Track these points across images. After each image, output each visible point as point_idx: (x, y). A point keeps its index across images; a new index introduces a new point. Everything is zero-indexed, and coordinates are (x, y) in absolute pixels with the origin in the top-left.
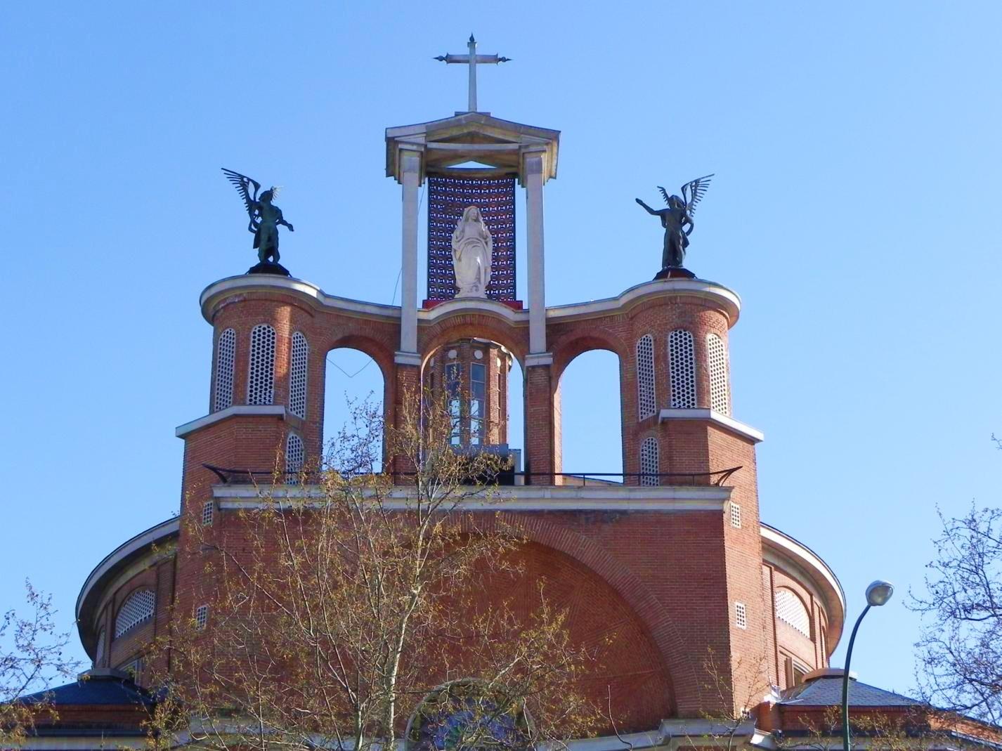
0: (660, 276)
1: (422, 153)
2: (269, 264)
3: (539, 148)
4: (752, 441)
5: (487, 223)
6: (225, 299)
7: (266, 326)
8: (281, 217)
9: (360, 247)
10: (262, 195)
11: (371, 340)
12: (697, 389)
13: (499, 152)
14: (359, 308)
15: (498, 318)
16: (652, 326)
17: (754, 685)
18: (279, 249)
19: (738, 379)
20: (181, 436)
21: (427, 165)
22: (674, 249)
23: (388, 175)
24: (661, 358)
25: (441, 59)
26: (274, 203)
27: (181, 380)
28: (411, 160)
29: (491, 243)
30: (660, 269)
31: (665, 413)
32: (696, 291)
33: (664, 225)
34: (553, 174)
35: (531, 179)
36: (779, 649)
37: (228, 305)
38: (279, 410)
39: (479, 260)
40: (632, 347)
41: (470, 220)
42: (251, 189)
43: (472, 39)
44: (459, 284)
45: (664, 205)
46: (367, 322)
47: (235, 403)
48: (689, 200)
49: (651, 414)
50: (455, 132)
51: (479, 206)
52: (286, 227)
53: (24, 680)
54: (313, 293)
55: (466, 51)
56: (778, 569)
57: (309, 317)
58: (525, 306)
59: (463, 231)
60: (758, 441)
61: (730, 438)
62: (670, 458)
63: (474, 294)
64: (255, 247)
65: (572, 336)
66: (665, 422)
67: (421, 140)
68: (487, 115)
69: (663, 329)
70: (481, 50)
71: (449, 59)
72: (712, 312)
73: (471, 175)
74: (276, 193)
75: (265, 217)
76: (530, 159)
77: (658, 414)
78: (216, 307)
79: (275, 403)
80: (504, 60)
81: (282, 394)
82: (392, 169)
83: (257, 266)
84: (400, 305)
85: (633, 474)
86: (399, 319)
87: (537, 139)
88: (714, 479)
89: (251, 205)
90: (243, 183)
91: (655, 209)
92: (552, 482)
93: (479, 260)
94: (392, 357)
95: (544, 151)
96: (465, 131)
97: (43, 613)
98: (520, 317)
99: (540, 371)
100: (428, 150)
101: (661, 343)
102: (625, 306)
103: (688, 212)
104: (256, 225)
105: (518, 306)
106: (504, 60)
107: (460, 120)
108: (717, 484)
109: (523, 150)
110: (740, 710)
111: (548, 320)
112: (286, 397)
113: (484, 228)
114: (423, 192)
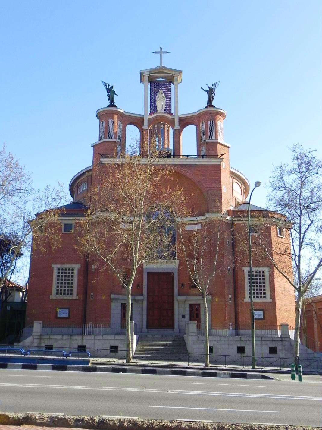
0: (207, 107)
1: (149, 77)
2: (112, 105)
3: (177, 75)
4: (228, 147)
5: (164, 94)
6: (102, 113)
7: (111, 120)
8: (115, 93)
9: (134, 100)
10: (110, 87)
11: (136, 123)
12: (215, 134)
13: (167, 76)
14: (134, 115)
15: (167, 118)
16: (204, 119)
17: (227, 205)
18: (115, 101)
19: (224, 132)
20: (92, 146)
21: (150, 80)
22: (210, 100)
23: (140, 82)
24: (206, 127)
25: (153, 52)
26: (113, 89)
27: (92, 133)
28: (146, 79)
29: (165, 99)
30: (207, 105)
31: (207, 141)
32: (215, 111)
33: (208, 94)
34: (181, 81)
35: (175, 83)
36: (233, 197)
37: (102, 115)
38: (115, 140)
39: (162, 103)
40: (199, 124)
41: (160, 94)
42: (108, 86)
43: (161, 47)
44: (158, 109)
45: (208, 89)
46: (136, 119)
47: (105, 138)
48: (214, 88)
49: (204, 141)
50: (157, 71)
51: (163, 90)
52: (116, 95)
53: (58, 204)
54: (123, 112)
55: (159, 50)
56: (234, 178)
57: (122, 118)
58: (174, 115)
59: (159, 96)
60: (230, 147)
61: (223, 147)
62: (208, 152)
63: (161, 112)
64: (109, 100)
65: (185, 122)
66: (207, 143)
67: (149, 73)
68: (164, 67)
69: (207, 120)
70: (163, 50)
71: (155, 52)
72: (219, 116)
73: (160, 82)
74: (113, 87)
75: (111, 93)
76: (175, 78)
77: (206, 141)
78: (100, 115)
79: (114, 138)
80: (169, 52)
81: (116, 136)
82: (142, 81)
83: (109, 105)
84: (143, 114)
85: (199, 155)
86: (143, 118)
87: (177, 73)
88: (219, 157)
89: (108, 90)
90: (106, 84)
91: (206, 90)
92: (180, 157)
93: (162, 103)
94: (142, 127)
95: (179, 76)
96: (159, 71)
97: (62, 188)
98: (173, 117)
99: (177, 130)
101: (206, 124)
102: (198, 114)
103: (214, 91)
104: (109, 95)
105: (172, 114)
106: (169, 52)
107: (158, 68)
108: (219, 158)
109: (173, 76)
110: (224, 210)
111: (179, 118)
112: (117, 137)
113: (163, 95)
114: (149, 86)
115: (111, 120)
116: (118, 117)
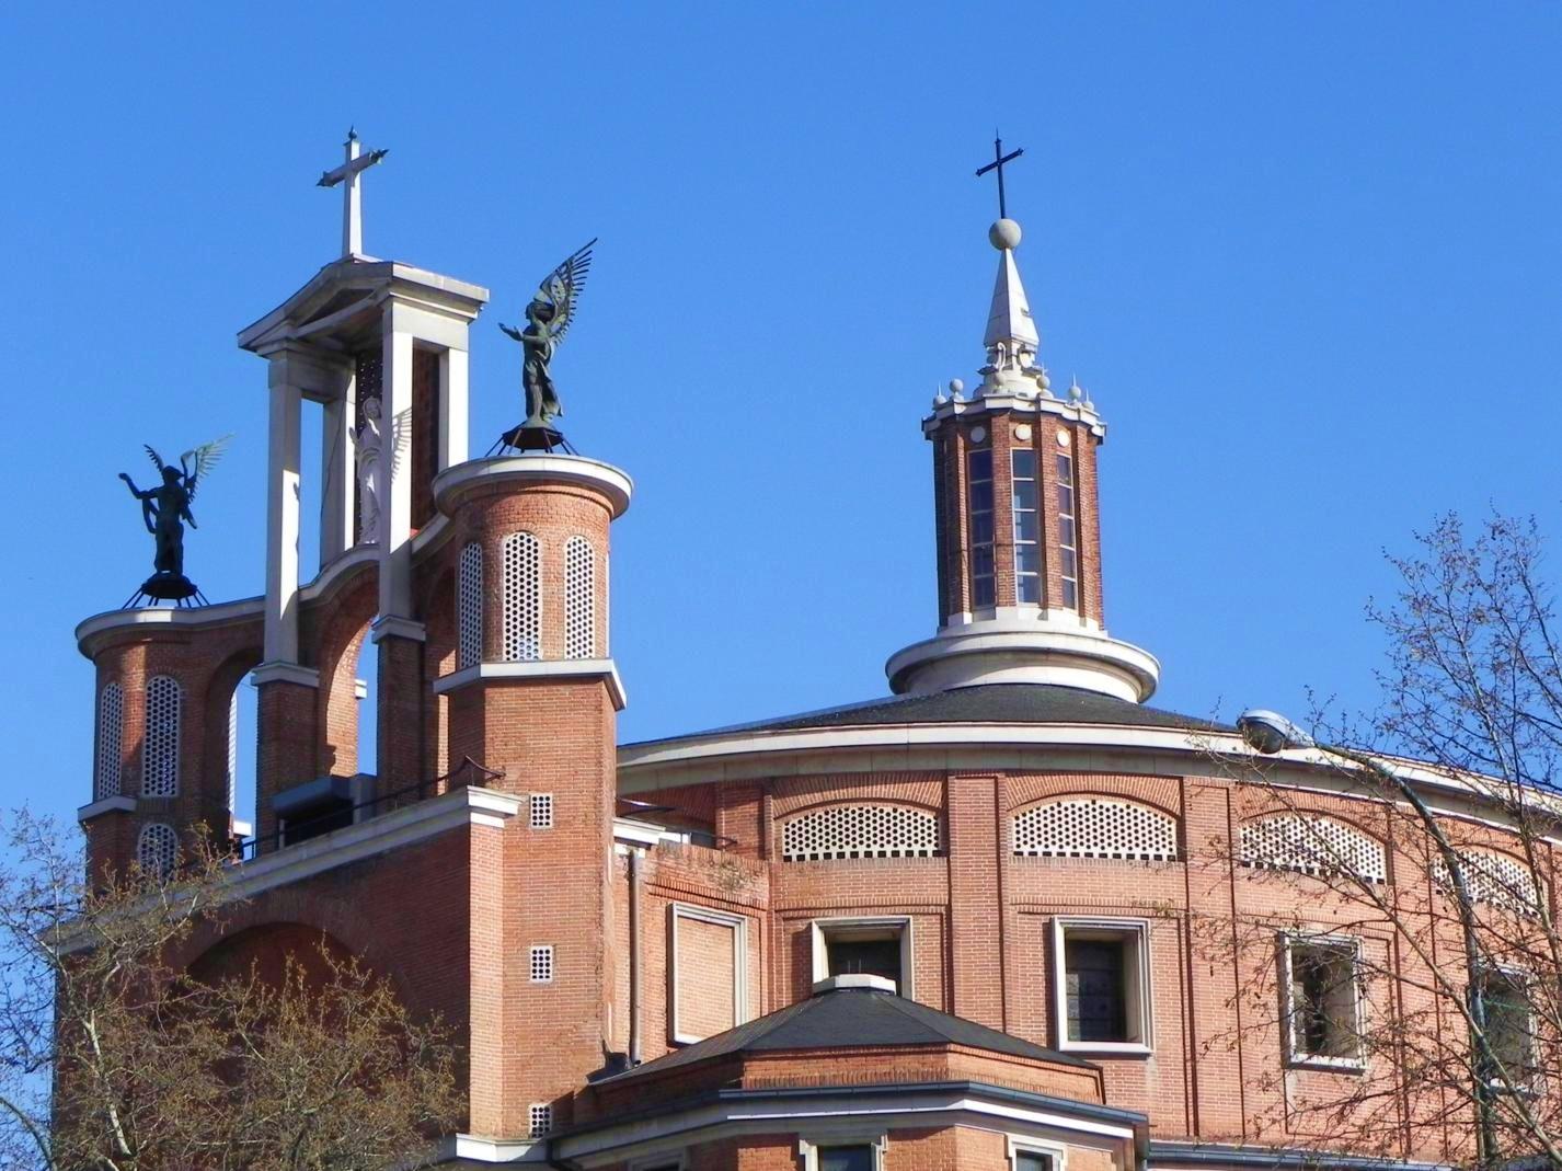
14: (235, 612)
50: (324, 300)
67: (284, 331)
72: (513, 499)
80: (380, 154)
86: (262, 613)
100: (303, 339)
115: (113, 684)
116: (147, 654)
